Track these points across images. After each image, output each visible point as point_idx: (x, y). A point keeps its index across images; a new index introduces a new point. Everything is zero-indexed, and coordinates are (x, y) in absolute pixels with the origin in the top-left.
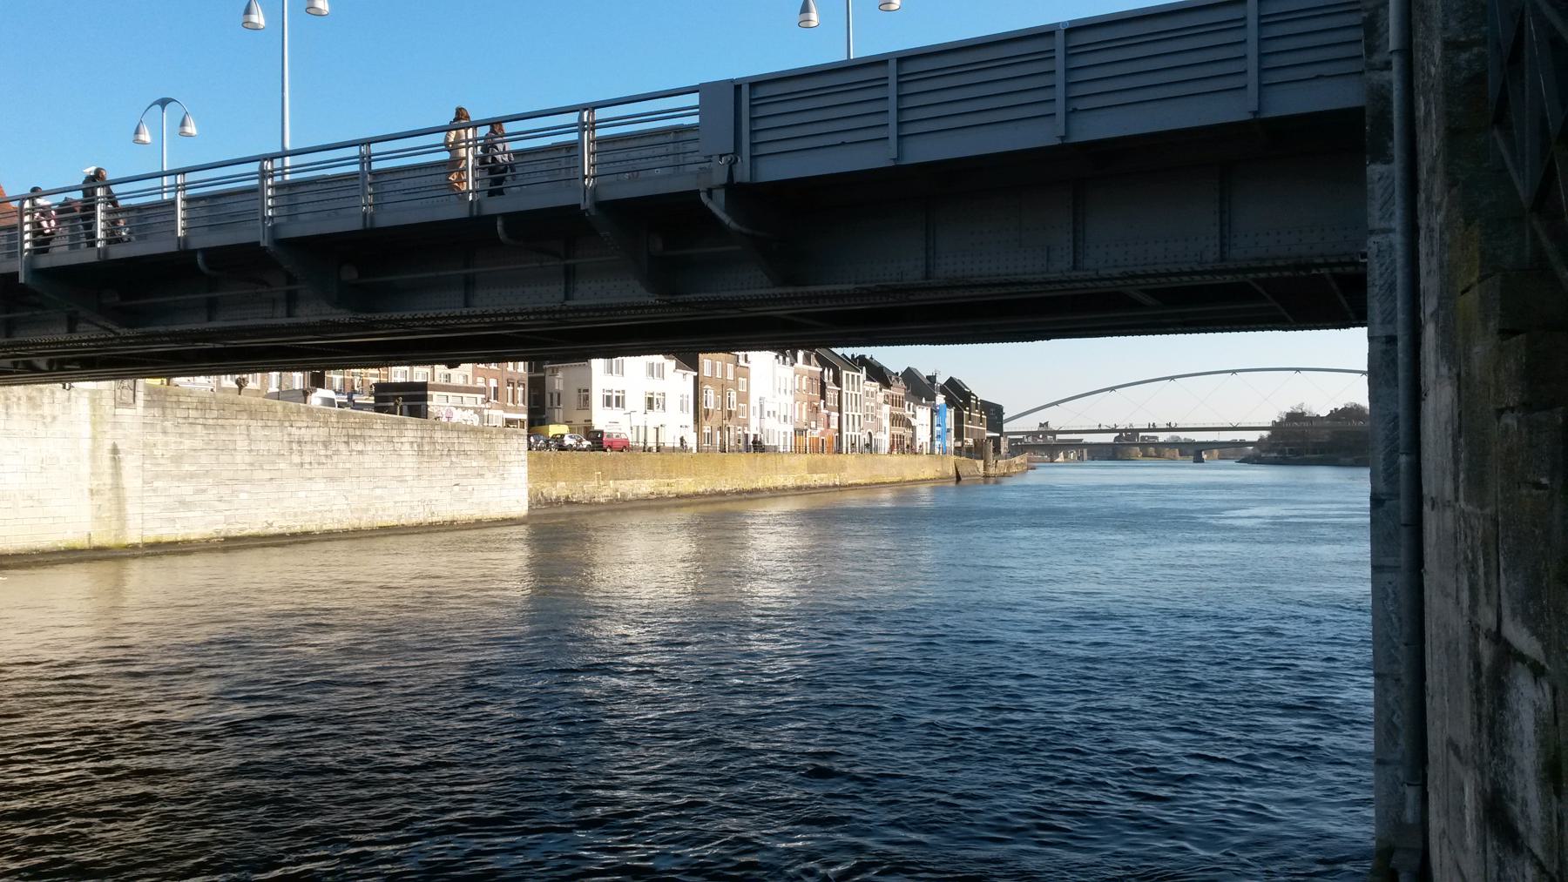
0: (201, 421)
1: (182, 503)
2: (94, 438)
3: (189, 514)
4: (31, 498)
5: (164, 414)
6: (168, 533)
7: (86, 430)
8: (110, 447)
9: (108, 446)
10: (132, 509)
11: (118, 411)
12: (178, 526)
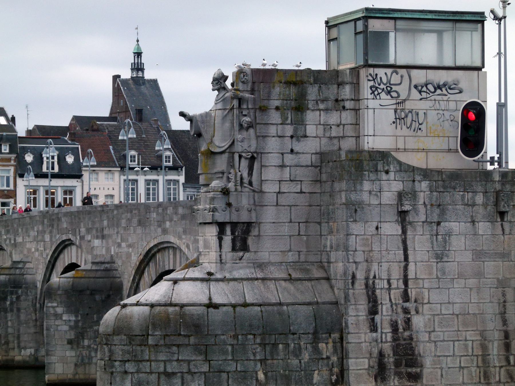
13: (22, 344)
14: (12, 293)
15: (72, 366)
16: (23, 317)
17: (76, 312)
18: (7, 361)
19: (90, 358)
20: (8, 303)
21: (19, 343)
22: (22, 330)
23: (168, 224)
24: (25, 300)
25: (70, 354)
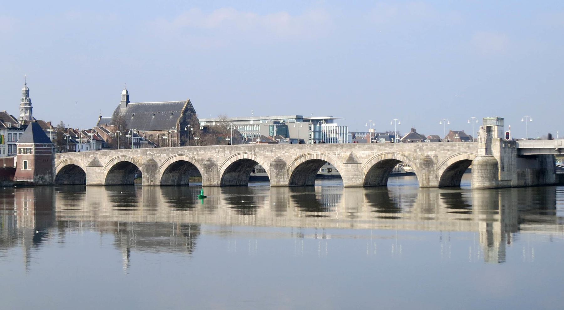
13: (214, 180)
14: (212, 167)
15: (276, 182)
16: (214, 173)
17: (277, 170)
18: (211, 185)
19: (280, 180)
20: (211, 169)
21: (213, 180)
22: (214, 176)
23: (317, 149)
24: (215, 169)
25: (276, 179)
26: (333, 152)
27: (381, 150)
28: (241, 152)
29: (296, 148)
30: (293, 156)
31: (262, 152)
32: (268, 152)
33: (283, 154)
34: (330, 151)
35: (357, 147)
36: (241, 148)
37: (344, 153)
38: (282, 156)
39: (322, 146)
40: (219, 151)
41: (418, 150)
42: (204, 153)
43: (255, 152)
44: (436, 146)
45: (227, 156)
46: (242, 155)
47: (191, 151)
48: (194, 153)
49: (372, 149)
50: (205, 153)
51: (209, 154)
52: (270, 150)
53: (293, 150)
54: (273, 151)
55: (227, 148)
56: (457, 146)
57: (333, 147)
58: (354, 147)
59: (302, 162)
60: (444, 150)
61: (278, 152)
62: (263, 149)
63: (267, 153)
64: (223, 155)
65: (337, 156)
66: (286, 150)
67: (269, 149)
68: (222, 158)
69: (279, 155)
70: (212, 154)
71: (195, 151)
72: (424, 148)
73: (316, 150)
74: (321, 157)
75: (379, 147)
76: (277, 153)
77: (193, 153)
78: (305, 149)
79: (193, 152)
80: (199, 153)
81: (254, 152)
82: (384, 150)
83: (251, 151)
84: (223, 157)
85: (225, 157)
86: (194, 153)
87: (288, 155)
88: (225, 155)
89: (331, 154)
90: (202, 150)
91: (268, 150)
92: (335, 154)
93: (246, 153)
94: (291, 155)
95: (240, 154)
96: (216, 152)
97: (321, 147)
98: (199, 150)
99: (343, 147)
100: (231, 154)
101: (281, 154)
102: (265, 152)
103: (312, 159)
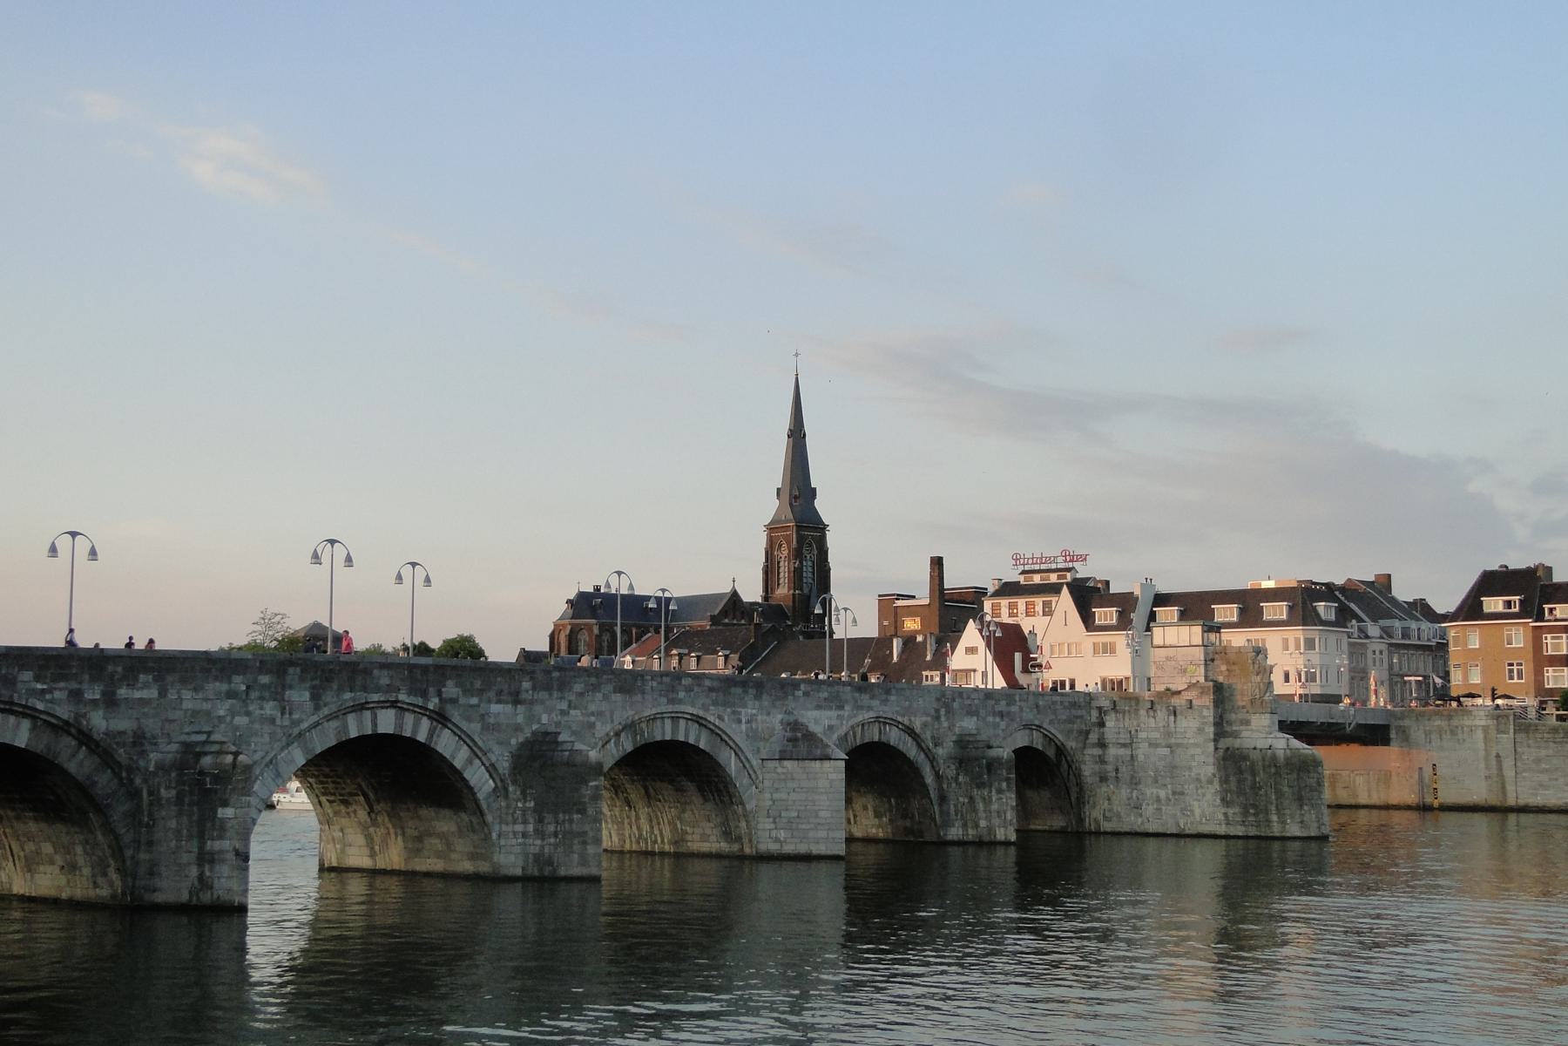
0: (1551, 740)
1: (1541, 785)
2: (1486, 750)
3: (1547, 792)
4: (1454, 778)
5: (1528, 737)
6: (1538, 800)
7: (1481, 745)
8: (1495, 755)
9: (1494, 753)
10: (1510, 788)
11: (1498, 736)
12: (1539, 798)
23: (681, 695)
26: (734, 713)
27: (861, 708)
28: (375, 697)
29: (610, 688)
30: (598, 724)
31: (474, 701)
32: (499, 702)
33: (563, 713)
34: (726, 704)
35: (800, 693)
36: (376, 672)
37: (765, 717)
38: (558, 724)
39: (699, 685)
40: (248, 687)
41: (943, 711)
42: (153, 693)
43: (441, 700)
44: (979, 699)
45: (296, 716)
46: (367, 714)
47: (64, 678)
48: (88, 696)
49: (841, 708)
50: (163, 693)
51: (187, 705)
52: (510, 694)
53: (599, 696)
54: (524, 696)
55: (298, 669)
56: (1018, 703)
57: (733, 690)
58: (793, 695)
59: (621, 754)
60: (994, 714)
61: (542, 702)
62: (478, 684)
63: (496, 708)
64: (270, 708)
65: (744, 727)
66: (573, 698)
67: (505, 687)
68: (267, 729)
69: (545, 719)
70: (206, 706)
71: (93, 680)
72: (956, 705)
73: (680, 702)
74: (687, 730)
75: (857, 695)
76: (538, 708)
77: (76, 695)
78: (643, 693)
79: (74, 685)
80: (123, 692)
81: (436, 700)
82: (870, 708)
83: (424, 694)
84: (272, 721)
85: (286, 723)
86: (88, 696)
87: (581, 718)
88: (283, 714)
89: (726, 718)
90: (142, 677)
91: (500, 692)
92: (740, 721)
93: (394, 704)
94: (593, 719)
95: (360, 708)
96: (231, 695)
97: (696, 689)
98: (124, 677)
99: (761, 694)
100: (317, 708)
101: (553, 715)
102: (489, 701)
103: (659, 738)
